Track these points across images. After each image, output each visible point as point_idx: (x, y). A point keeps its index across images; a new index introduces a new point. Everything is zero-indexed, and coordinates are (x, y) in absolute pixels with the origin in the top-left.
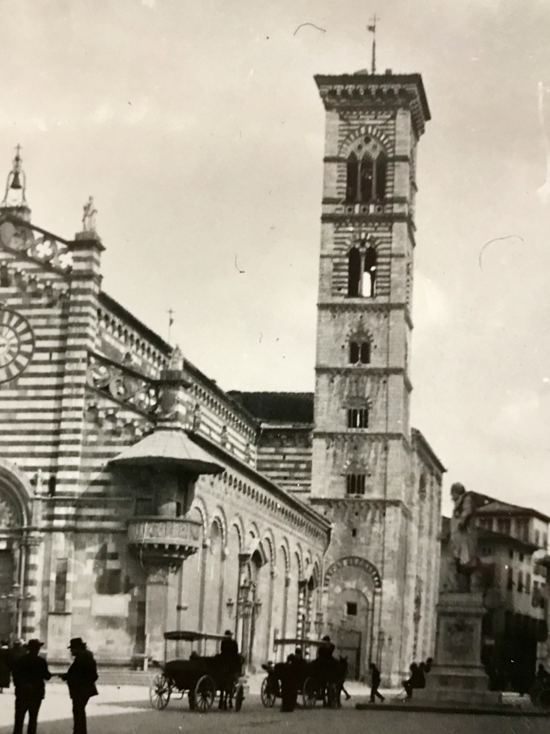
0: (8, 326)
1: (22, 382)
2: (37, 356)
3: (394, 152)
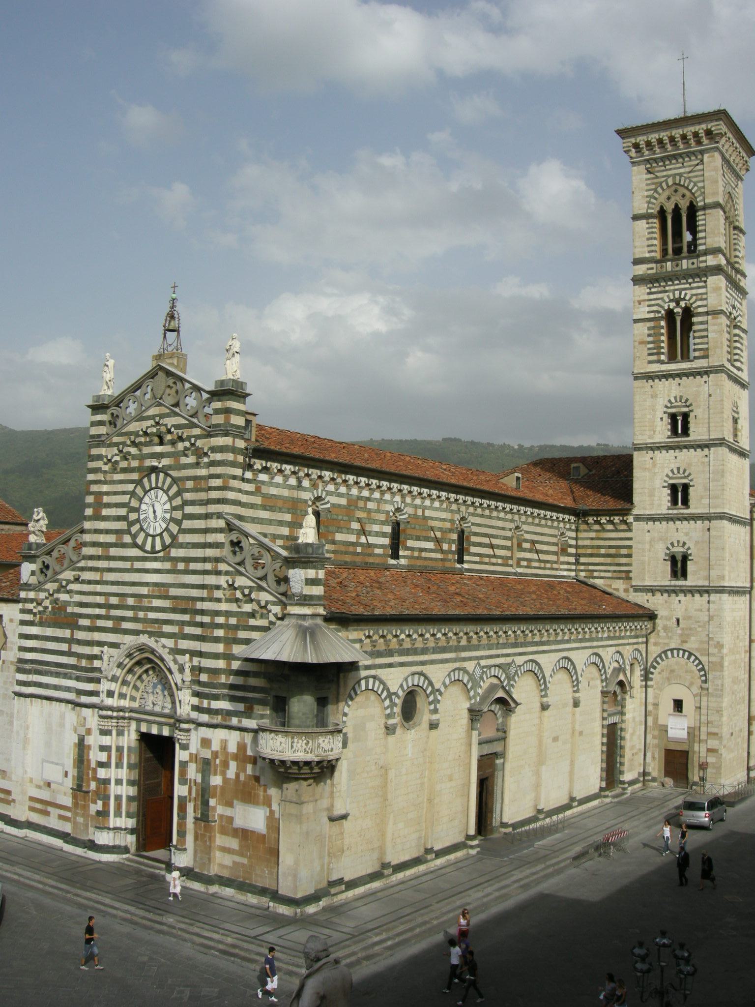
0: (162, 489)
1: (174, 553)
2: (187, 524)
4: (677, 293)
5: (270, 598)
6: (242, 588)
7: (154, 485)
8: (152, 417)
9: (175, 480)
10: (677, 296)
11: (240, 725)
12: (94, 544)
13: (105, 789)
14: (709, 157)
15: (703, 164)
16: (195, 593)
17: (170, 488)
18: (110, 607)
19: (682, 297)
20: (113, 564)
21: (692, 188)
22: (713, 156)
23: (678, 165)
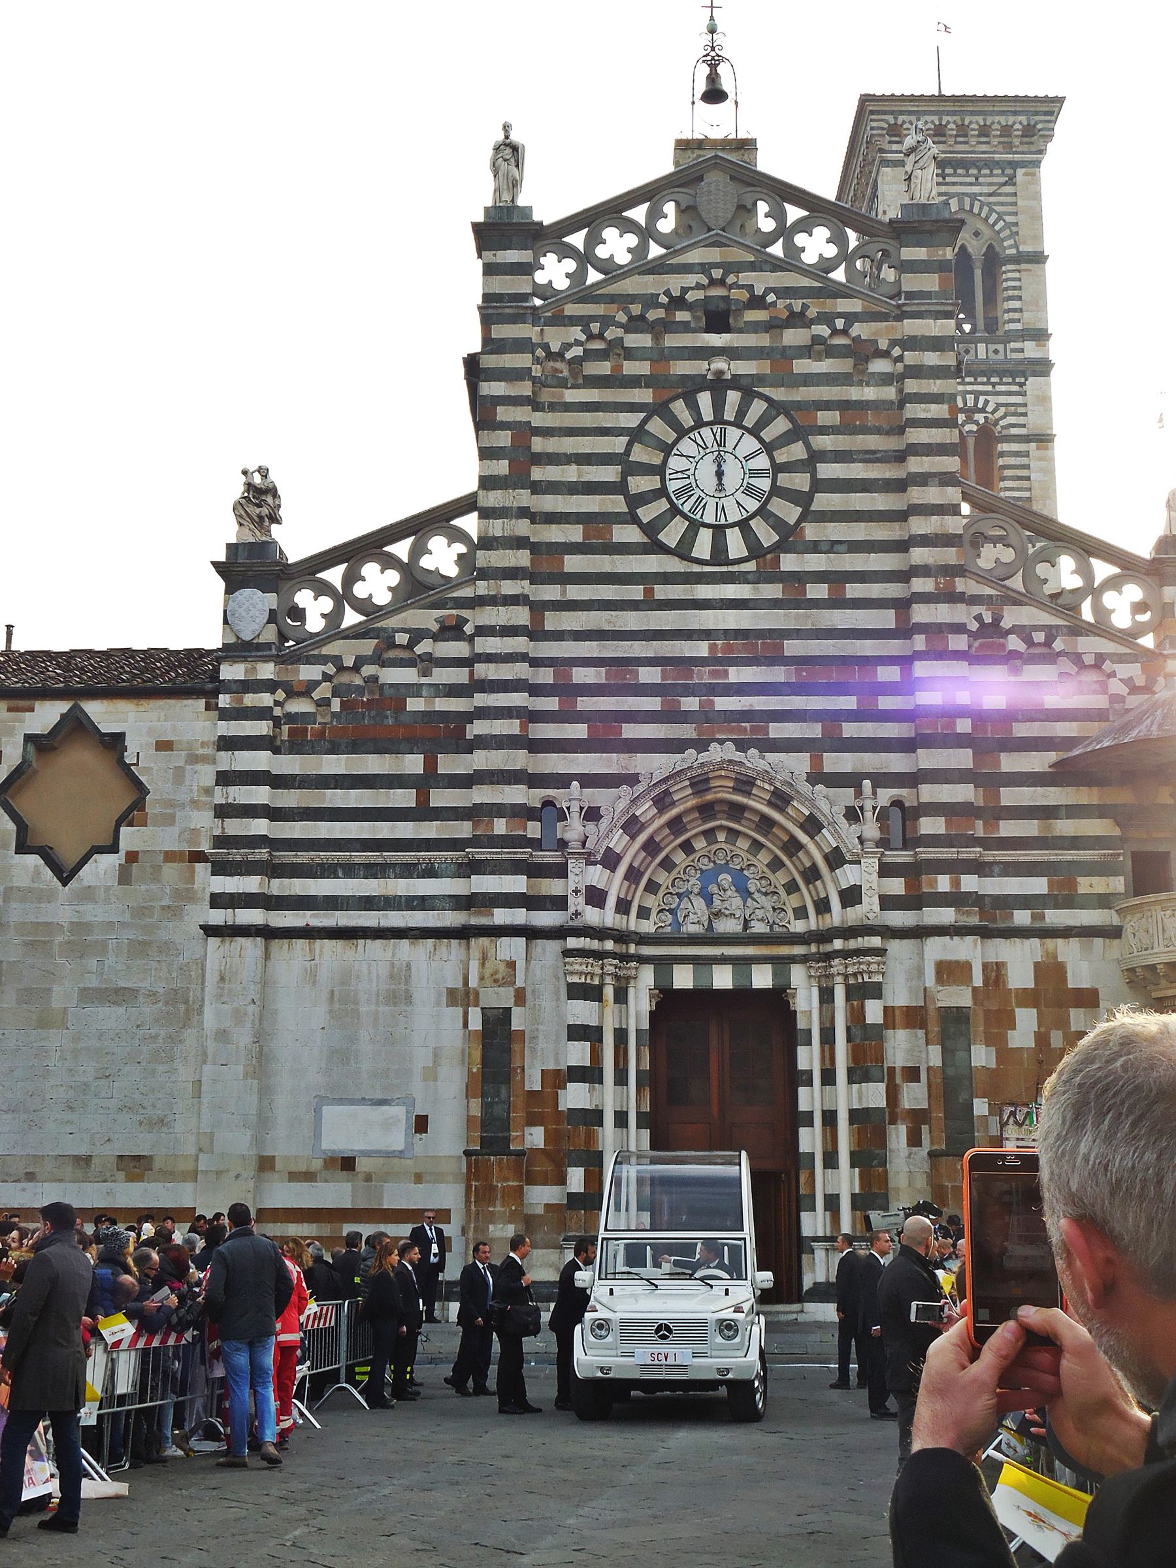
0: (738, 424)
1: (789, 563)
2: (823, 501)
3: (1016, 246)
4: (970, 399)
5: (1107, 646)
6: (1024, 632)
7: (707, 414)
8: (705, 268)
9: (776, 408)
10: (970, 403)
11: (1037, 925)
12: (520, 543)
13: (591, 1138)
14: (1026, 174)
15: (1015, 184)
16: (867, 648)
17: (764, 422)
18: (567, 690)
19: (980, 405)
20: (575, 592)
21: (995, 223)
22: (1034, 174)
23: (968, 180)
